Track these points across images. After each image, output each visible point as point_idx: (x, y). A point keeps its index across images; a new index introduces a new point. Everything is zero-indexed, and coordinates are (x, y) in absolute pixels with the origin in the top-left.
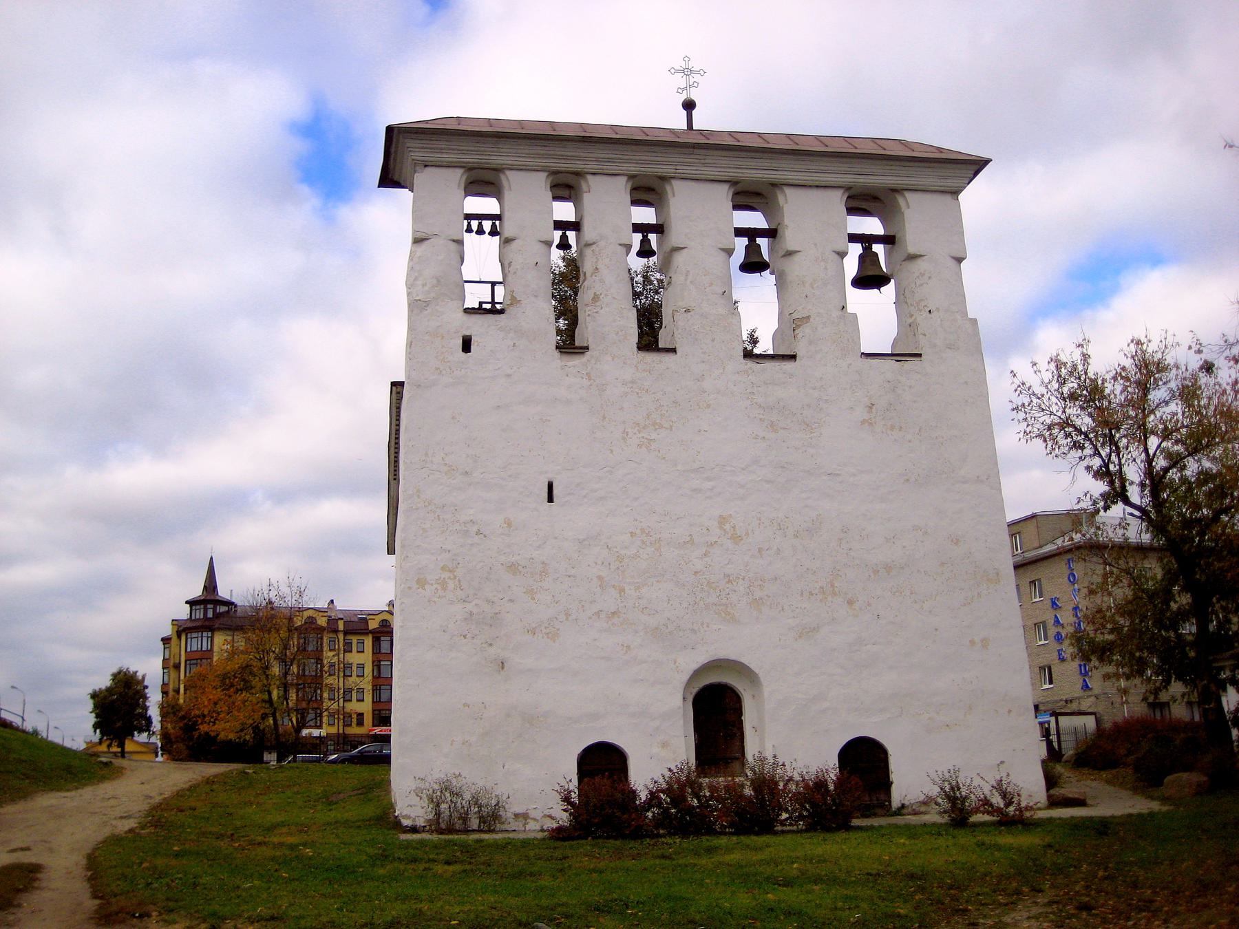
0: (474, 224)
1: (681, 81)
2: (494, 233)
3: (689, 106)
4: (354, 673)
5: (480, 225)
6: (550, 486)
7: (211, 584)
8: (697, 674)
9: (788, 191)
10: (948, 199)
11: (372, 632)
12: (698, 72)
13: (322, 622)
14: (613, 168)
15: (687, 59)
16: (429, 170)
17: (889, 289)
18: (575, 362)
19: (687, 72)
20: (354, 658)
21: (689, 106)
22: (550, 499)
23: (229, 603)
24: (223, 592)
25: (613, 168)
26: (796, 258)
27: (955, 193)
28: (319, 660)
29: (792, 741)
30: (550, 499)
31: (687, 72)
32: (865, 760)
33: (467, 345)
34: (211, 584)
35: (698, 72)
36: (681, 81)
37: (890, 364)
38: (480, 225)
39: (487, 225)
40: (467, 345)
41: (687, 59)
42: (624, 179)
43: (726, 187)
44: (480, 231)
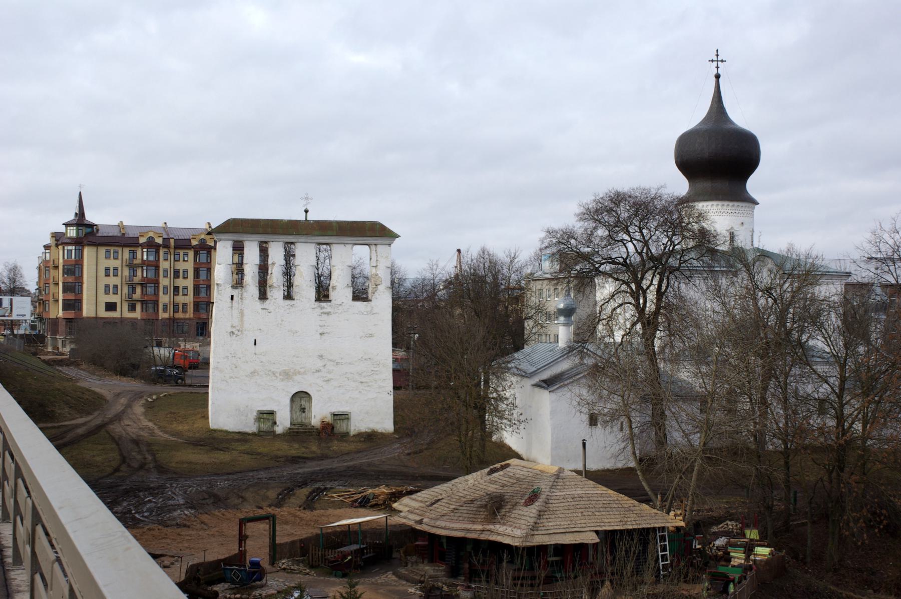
3: (306, 211)
4: (181, 259)
7: (81, 214)
11: (194, 247)
13: (159, 241)
15: (307, 194)
19: (307, 199)
20: (181, 266)
21: (306, 211)
23: (92, 226)
24: (91, 217)
27: (390, 245)
28: (157, 267)
29: (318, 414)
31: (307, 199)
33: (232, 297)
34: (81, 214)
36: (304, 202)
40: (232, 297)
41: (307, 194)
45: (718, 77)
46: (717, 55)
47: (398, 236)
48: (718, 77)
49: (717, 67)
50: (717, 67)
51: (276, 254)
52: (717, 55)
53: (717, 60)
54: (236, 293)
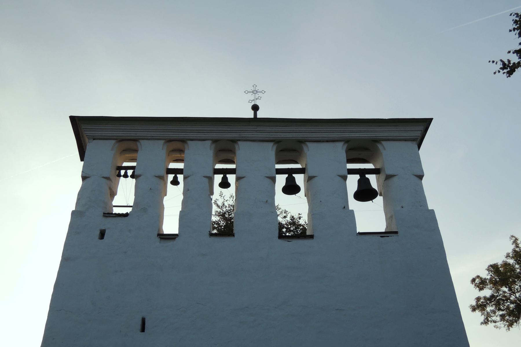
0: (123, 172)
2: (133, 176)
3: (255, 108)
5: (126, 173)
9: (309, 144)
12: (261, 92)
15: (255, 86)
16: (95, 141)
17: (379, 200)
22: (143, 330)
30: (143, 330)
33: (102, 234)
35: (261, 92)
36: (251, 97)
37: (378, 237)
38: (126, 173)
39: (130, 172)
40: (102, 234)
42: (209, 143)
43: (271, 144)
44: (126, 176)
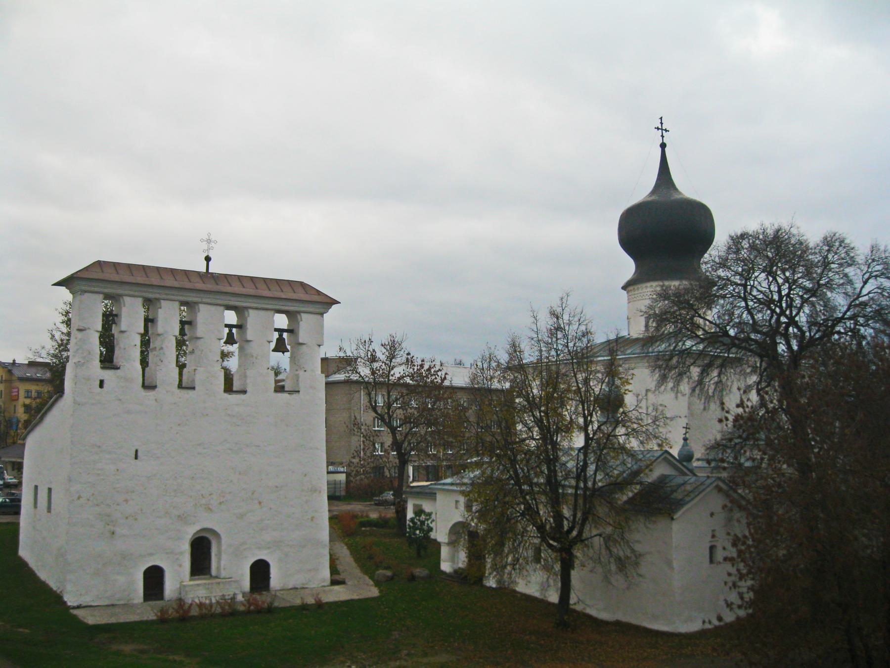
1: (205, 246)
3: (208, 259)
6: (137, 451)
8: (195, 534)
10: (319, 317)
14: (173, 297)
15: (209, 234)
18: (151, 394)
19: (209, 241)
21: (208, 259)
22: (136, 458)
25: (173, 297)
26: (251, 343)
27: (322, 314)
30: (136, 458)
32: (260, 571)
33: (102, 384)
36: (205, 246)
40: (102, 384)
41: (209, 234)
45: (663, 146)
46: (662, 123)
47: (332, 302)
48: (663, 146)
49: (663, 136)
50: (663, 136)
51: (169, 318)
52: (662, 123)
53: (661, 129)
54: (107, 375)
